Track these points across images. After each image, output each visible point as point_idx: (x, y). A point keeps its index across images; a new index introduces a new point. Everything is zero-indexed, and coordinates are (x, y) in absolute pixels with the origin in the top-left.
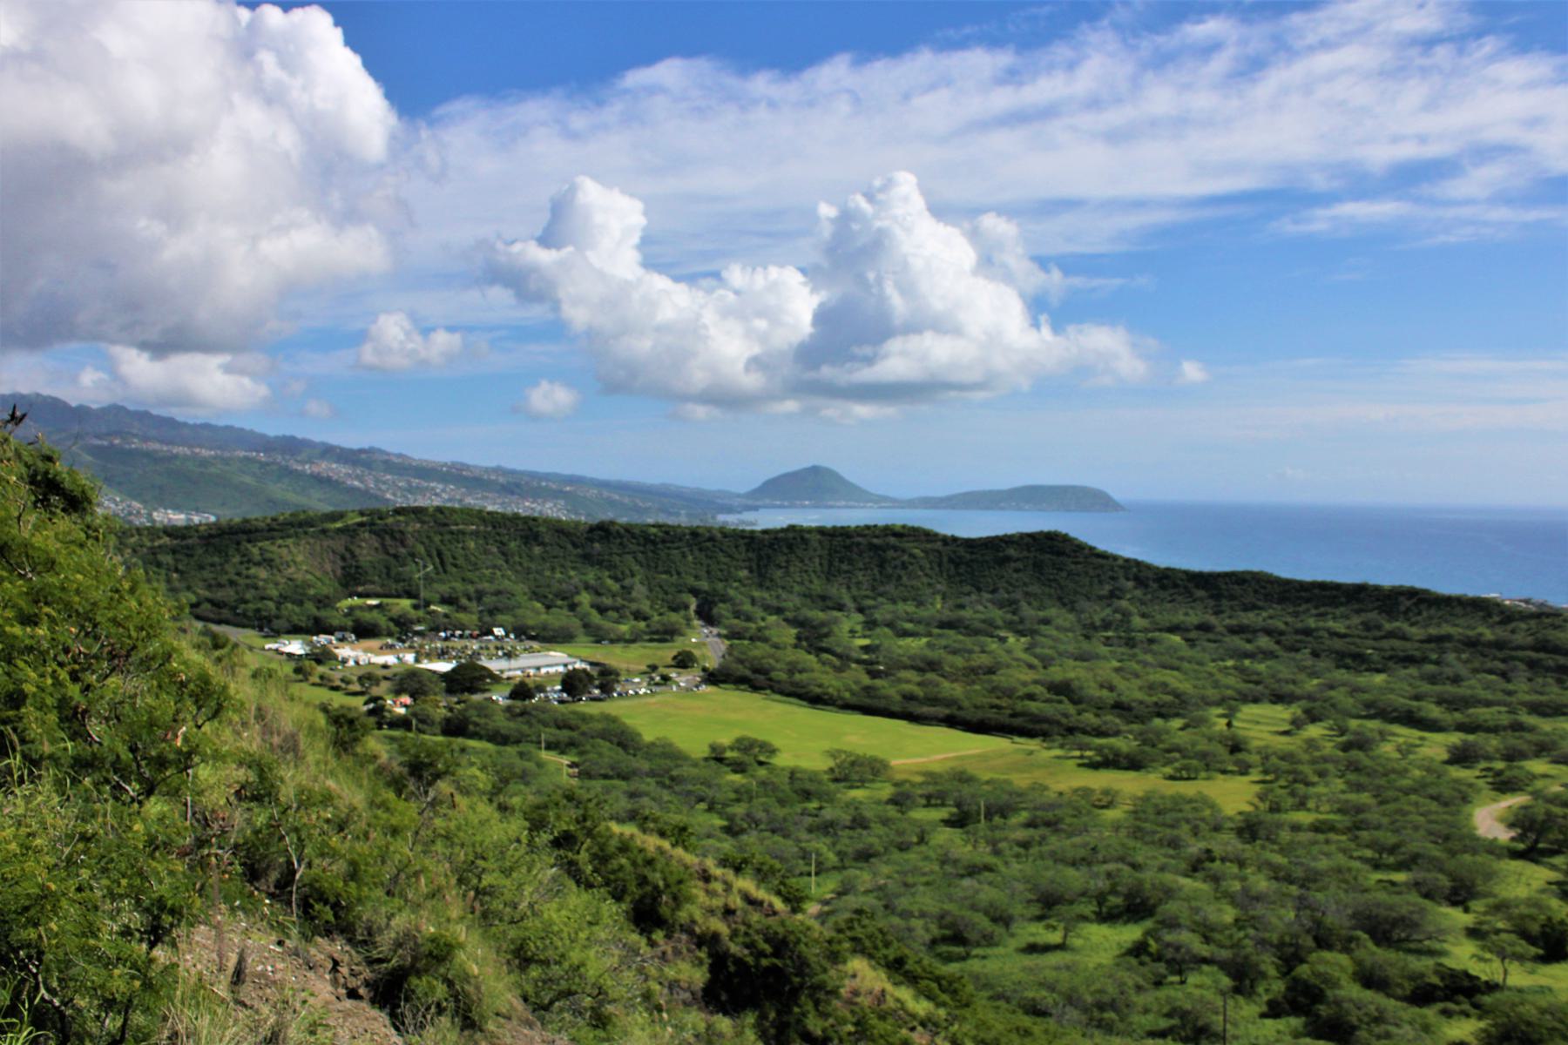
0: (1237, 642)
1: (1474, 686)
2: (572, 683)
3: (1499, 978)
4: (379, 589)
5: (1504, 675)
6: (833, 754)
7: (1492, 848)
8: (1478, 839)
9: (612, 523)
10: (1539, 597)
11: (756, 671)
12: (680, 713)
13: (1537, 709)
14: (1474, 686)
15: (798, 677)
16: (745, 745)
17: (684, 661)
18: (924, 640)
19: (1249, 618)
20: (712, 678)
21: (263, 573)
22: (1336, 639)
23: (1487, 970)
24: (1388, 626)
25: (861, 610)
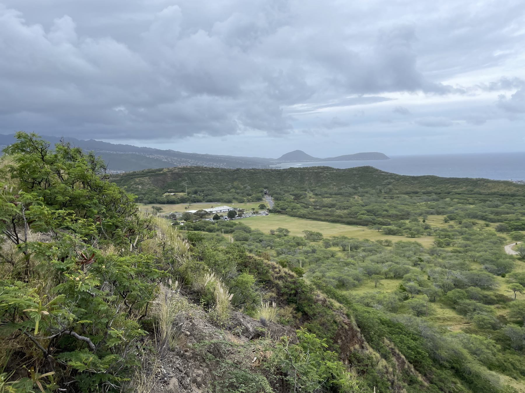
0: (425, 197)
1: (503, 208)
2: (232, 215)
3: (513, 297)
4: (174, 190)
5: (513, 204)
6: (306, 232)
7: (511, 257)
8: (506, 255)
9: (240, 169)
11: (282, 209)
12: (263, 222)
14: (503, 208)
15: (294, 210)
16: (280, 230)
17: (262, 207)
18: (331, 199)
19: (430, 189)
20: (270, 211)
21: (140, 187)
22: (457, 195)
23: (510, 294)
25: (312, 191)
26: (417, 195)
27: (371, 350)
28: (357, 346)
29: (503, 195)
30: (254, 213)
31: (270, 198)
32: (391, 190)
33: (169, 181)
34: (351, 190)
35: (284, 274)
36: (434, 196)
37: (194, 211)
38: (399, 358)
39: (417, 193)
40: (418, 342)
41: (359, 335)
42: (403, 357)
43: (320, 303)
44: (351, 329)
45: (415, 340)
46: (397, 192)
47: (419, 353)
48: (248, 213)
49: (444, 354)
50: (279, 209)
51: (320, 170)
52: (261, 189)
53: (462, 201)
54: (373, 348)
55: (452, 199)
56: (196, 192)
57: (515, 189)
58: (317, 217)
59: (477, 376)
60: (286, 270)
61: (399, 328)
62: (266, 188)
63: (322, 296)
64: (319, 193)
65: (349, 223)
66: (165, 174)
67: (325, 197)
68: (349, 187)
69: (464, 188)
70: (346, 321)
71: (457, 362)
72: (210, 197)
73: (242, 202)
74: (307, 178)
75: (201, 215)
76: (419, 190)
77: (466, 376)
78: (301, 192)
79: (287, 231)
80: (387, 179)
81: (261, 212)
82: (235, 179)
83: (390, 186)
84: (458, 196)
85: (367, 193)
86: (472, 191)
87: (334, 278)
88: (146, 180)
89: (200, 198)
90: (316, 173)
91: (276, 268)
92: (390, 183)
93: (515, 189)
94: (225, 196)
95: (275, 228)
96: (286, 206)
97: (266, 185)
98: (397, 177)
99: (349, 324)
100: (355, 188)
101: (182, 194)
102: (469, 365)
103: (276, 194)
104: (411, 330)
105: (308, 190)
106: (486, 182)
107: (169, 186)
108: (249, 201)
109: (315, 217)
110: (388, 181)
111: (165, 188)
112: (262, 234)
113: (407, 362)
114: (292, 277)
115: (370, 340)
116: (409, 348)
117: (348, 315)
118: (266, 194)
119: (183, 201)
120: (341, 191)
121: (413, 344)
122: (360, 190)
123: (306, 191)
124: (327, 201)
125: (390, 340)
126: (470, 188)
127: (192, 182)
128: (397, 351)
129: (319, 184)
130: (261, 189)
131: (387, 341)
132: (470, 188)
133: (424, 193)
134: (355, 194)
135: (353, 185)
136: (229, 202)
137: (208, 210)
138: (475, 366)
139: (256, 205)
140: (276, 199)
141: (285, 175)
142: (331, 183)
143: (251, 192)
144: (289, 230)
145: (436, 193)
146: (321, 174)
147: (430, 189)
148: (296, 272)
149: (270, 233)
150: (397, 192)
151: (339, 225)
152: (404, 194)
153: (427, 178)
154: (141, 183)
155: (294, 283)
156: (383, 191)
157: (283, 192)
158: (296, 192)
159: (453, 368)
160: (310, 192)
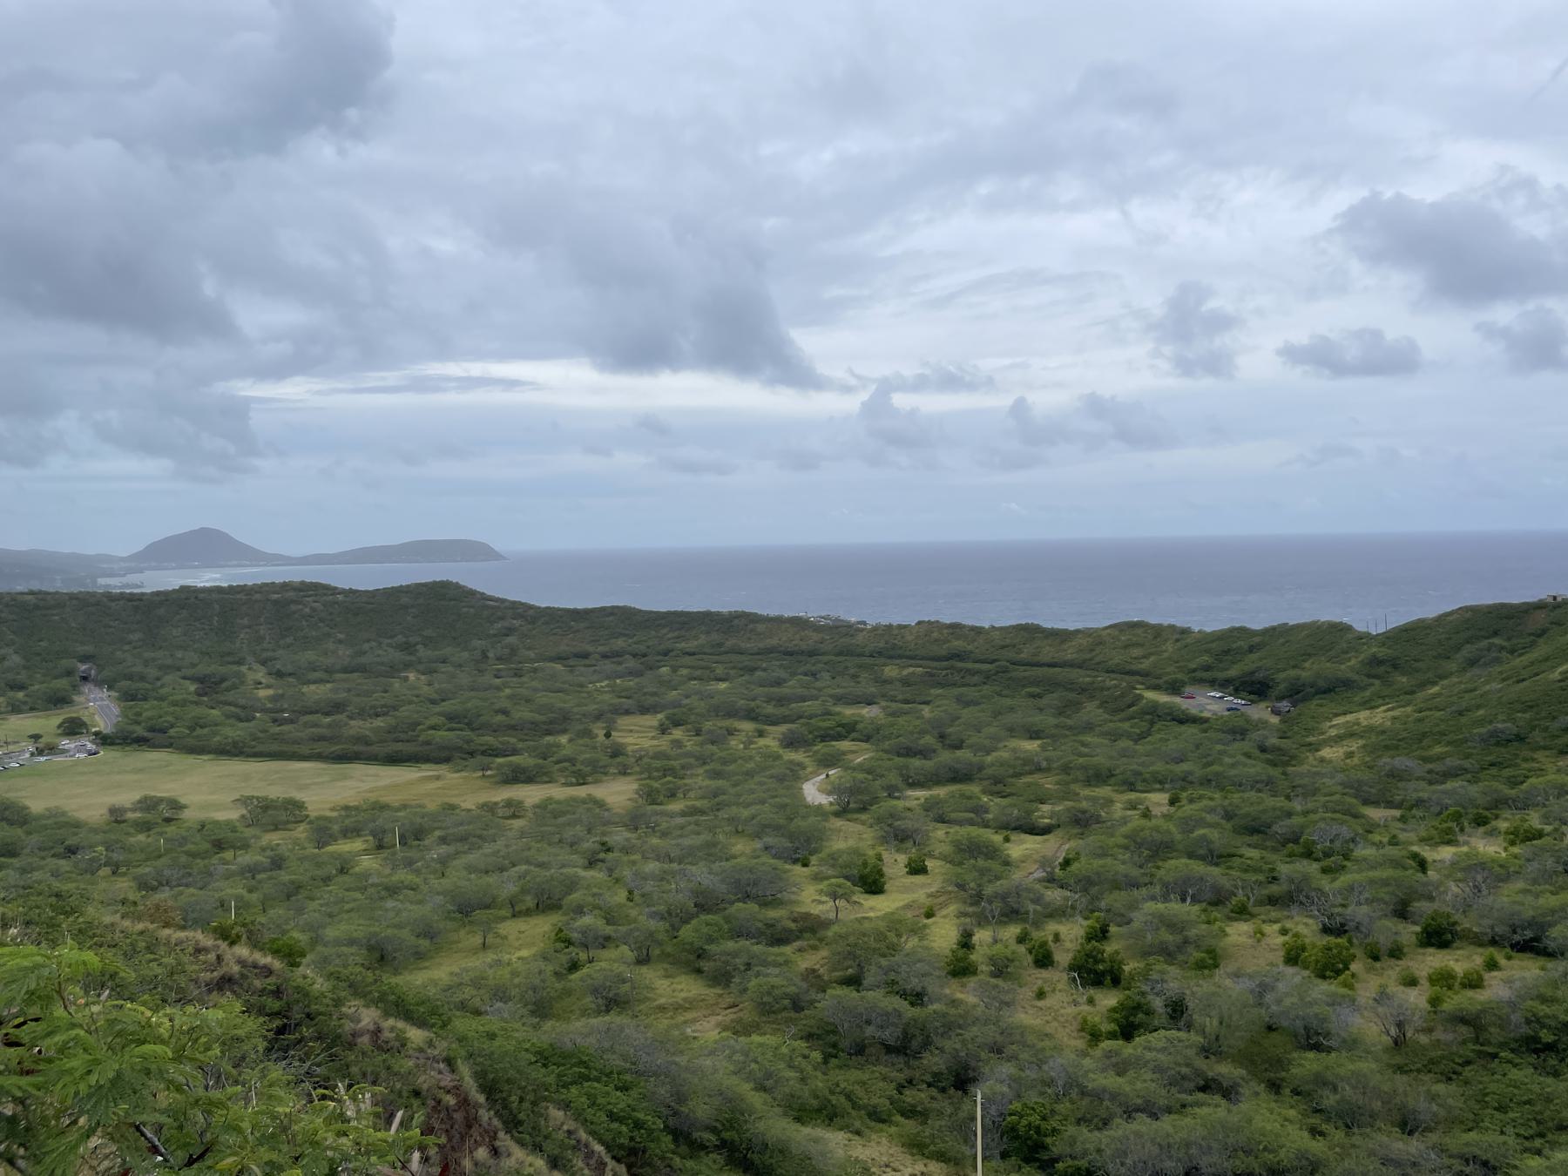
0: (608, 666)
5: (814, 675)
6: (244, 801)
10: (833, 614)
11: (152, 730)
13: (839, 699)
14: (792, 686)
15: (199, 731)
16: (148, 804)
17: (73, 728)
18: (329, 686)
20: (104, 740)
24: (729, 644)
25: (264, 663)
26: (587, 662)
27: (518, 1153)
28: (482, 1153)
29: (791, 654)
30: (40, 752)
31: (105, 693)
32: (514, 651)
34: (398, 656)
35: (236, 969)
36: (631, 663)
38: (590, 1154)
39: (585, 656)
40: (634, 1093)
41: (485, 1115)
42: (598, 1148)
43: (364, 1041)
44: (464, 1102)
45: (624, 1088)
46: (532, 654)
47: (638, 1125)
49: (701, 1110)
50: (140, 731)
51: (291, 594)
52: (65, 663)
53: (698, 673)
54: (522, 1144)
55: (674, 669)
57: (816, 636)
58: (285, 748)
59: (781, 1151)
60: (242, 951)
61: (582, 1063)
62: (85, 659)
63: (369, 1017)
64: (290, 669)
65: (393, 760)
67: (309, 682)
68: (389, 645)
69: (703, 639)
70: (447, 1080)
71: (731, 1124)
74: (246, 621)
76: (590, 648)
77: (755, 1157)
78: (223, 670)
79: (176, 805)
80: (502, 618)
81: (65, 743)
83: (511, 640)
84: (688, 660)
85: (444, 662)
86: (720, 645)
87: (1379, 1129)
90: (276, 602)
91: (206, 950)
92: (509, 631)
93: (816, 636)
95: (126, 798)
96: (170, 718)
97: (88, 649)
98: (531, 612)
99: (456, 1090)
100: (407, 648)
102: (761, 1126)
103: (130, 677)
104: (616, 1062)
105: (250, 659)
106: (752, 621)
109: (275, 747)
110: (506, 624)
112: (77, 825)
113: (608, 1159)
114: (268, 971)
115: (513, 1124)
116: (612, 1116)
117: (450, 1062)
118: (85, 679)
120: (363, 660)
121: (620, 1101)
122: (422, 652)
123: (240, 662)
124: (316, 692)
125: (566, 1106)
126: (715, 637)
128: (583, 1135)
129: (289, 640)
130: (65, 663)
131: (557, 1114)
132: (715, 637)
133: (605, 656)
134: (407, 666)
135: (400, 639)
138: (776, 1127)
140: (128, 697)
141: (161, 611)
142: (329, 635)
143: (22, 677)
144: (183, 801)
145: (634, 656)
146: (293, 607)
147: (620, 643)
148: (276, 952)
149: (107, 817)
150: (532, 654)
151: (358, 769)
152: (552, 659)
153: (612, 614)
155: (277, 993)
156: (491, 655)
157: (152, 672)
158: (203, 669)
159: (723, 1145)
160: (256, 666)
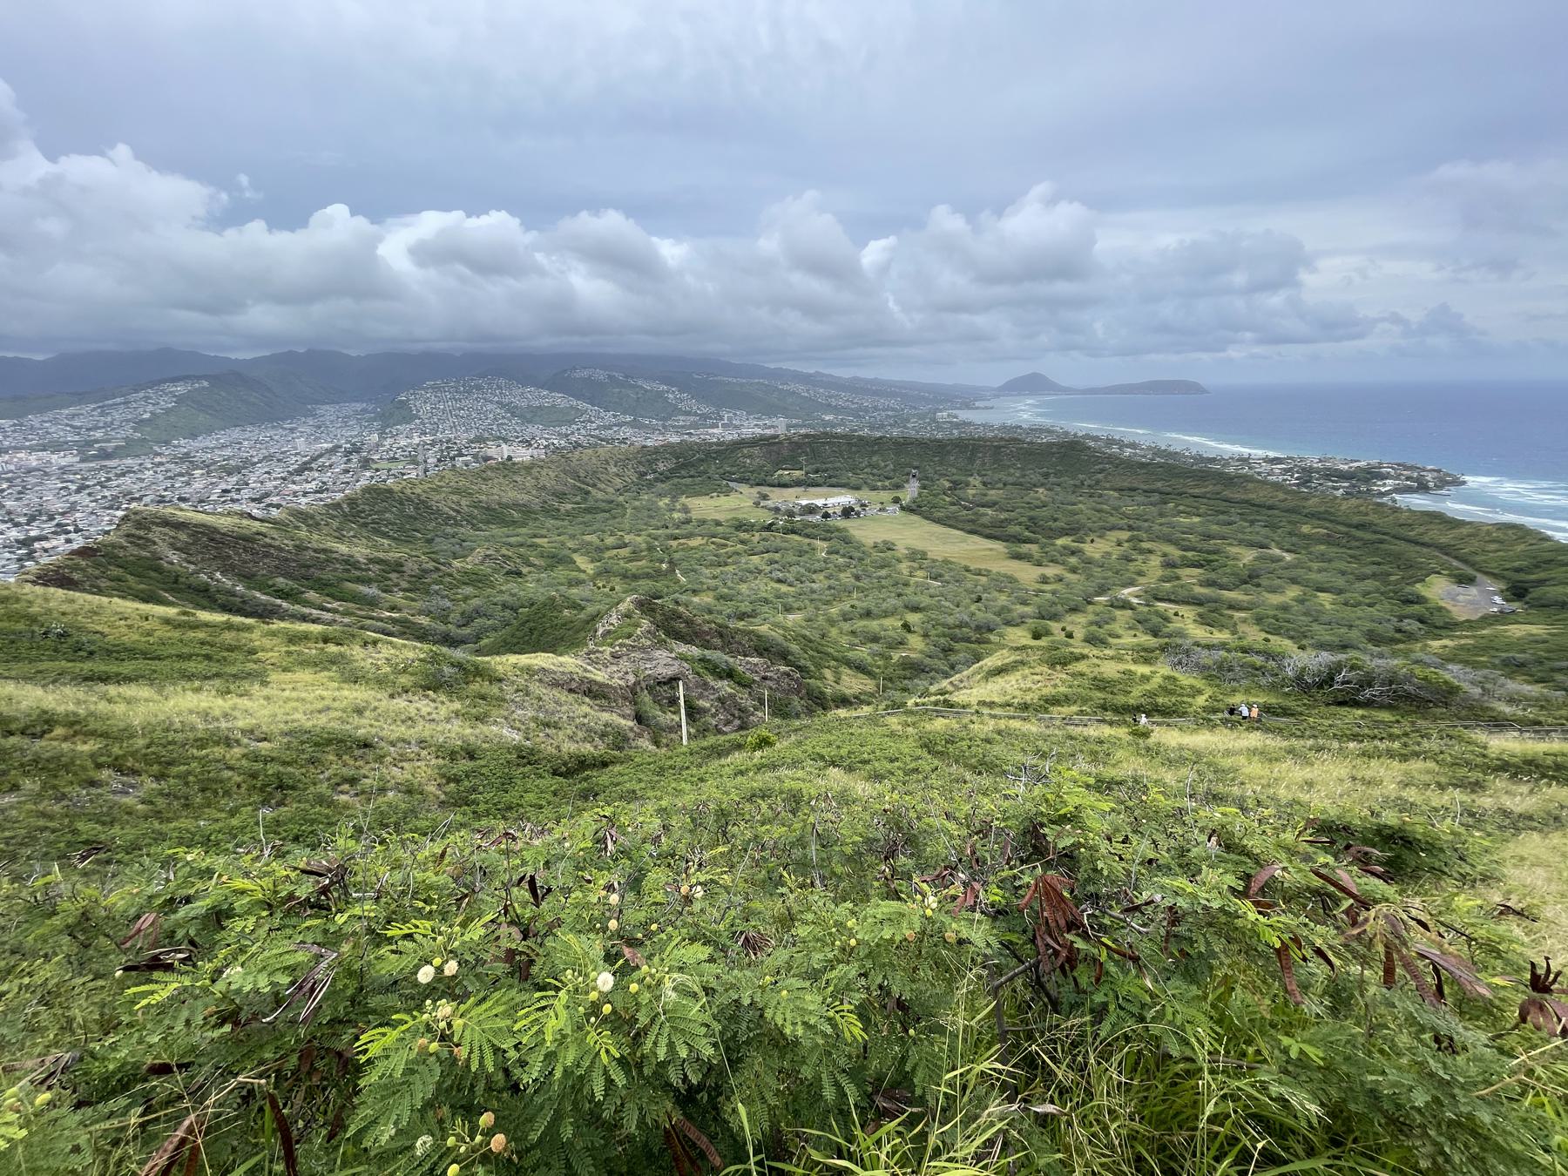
2: (847, 512)
16: (885, 542)
17: (896, 500)
19: (1159, 484)
20: (902, 508)
32: (1098, 482)
33: (785, 452)
36: (1156, 497)
37: (804, 502)
39: (1131, 489)
48: (873, 510)
56: (817, 472)
57: (1281, 496)
66: (780, 443)
72: (834, 480)
73: (874, 488)
75: (811, 510)
82: (874, 453)
83: (1100, 476)
88: (756, 451)
89: (821, 481)
92: (1101, 471)
93: (1281, 496)
94: (854, 480)
101: (797, 473)
107: (785, 461)
108: (884, 488)
111: (778, 465)
119: (798, 483)
124: (993, 494)
126: (1218, 488)
127: (815, 454)
134: (1042, 485)
136: (857, 488)
137: (820, 502)
139: (886, 496)
147: (1159, 484)
151: (975, 538)
154: (749, 457)
158: (955, 478)
